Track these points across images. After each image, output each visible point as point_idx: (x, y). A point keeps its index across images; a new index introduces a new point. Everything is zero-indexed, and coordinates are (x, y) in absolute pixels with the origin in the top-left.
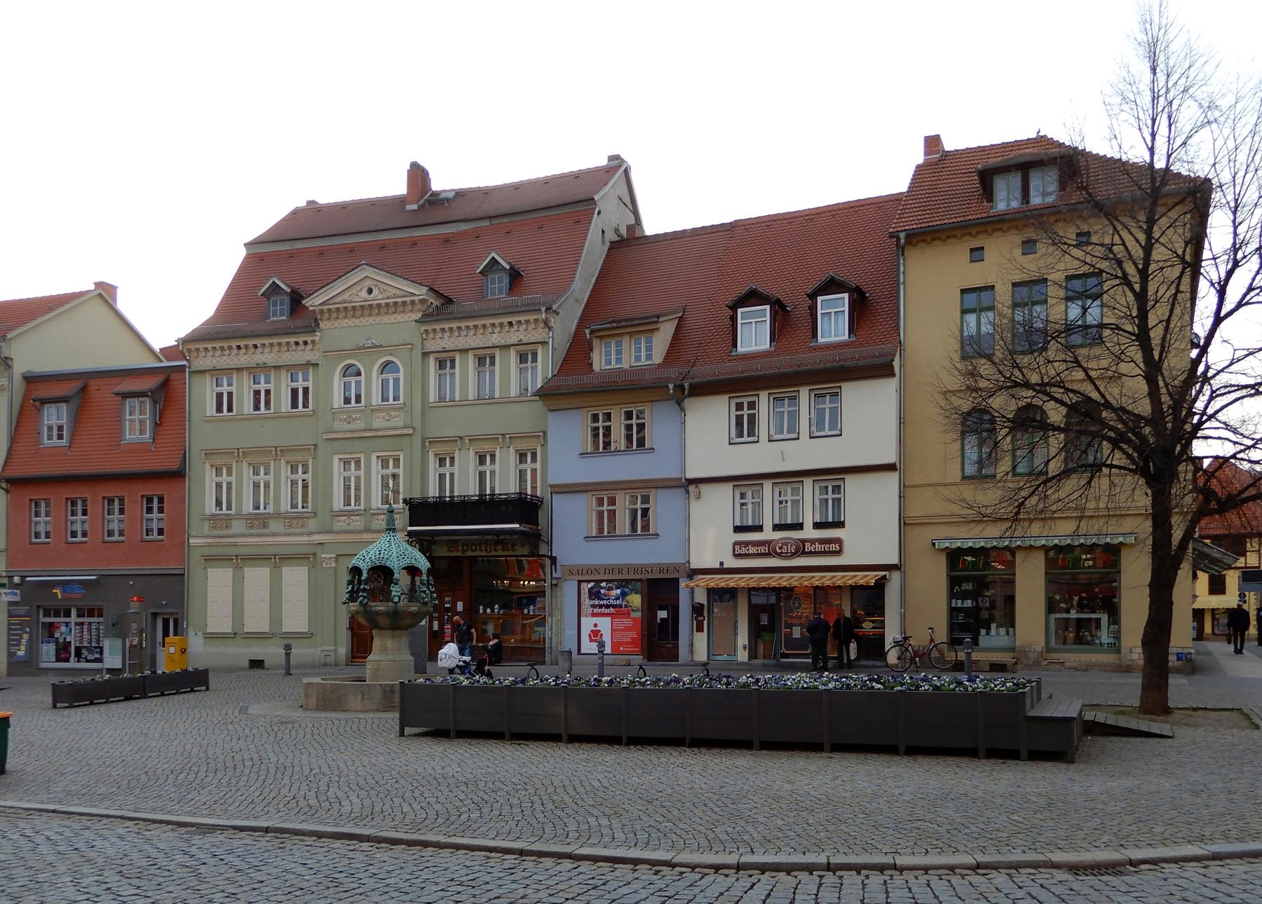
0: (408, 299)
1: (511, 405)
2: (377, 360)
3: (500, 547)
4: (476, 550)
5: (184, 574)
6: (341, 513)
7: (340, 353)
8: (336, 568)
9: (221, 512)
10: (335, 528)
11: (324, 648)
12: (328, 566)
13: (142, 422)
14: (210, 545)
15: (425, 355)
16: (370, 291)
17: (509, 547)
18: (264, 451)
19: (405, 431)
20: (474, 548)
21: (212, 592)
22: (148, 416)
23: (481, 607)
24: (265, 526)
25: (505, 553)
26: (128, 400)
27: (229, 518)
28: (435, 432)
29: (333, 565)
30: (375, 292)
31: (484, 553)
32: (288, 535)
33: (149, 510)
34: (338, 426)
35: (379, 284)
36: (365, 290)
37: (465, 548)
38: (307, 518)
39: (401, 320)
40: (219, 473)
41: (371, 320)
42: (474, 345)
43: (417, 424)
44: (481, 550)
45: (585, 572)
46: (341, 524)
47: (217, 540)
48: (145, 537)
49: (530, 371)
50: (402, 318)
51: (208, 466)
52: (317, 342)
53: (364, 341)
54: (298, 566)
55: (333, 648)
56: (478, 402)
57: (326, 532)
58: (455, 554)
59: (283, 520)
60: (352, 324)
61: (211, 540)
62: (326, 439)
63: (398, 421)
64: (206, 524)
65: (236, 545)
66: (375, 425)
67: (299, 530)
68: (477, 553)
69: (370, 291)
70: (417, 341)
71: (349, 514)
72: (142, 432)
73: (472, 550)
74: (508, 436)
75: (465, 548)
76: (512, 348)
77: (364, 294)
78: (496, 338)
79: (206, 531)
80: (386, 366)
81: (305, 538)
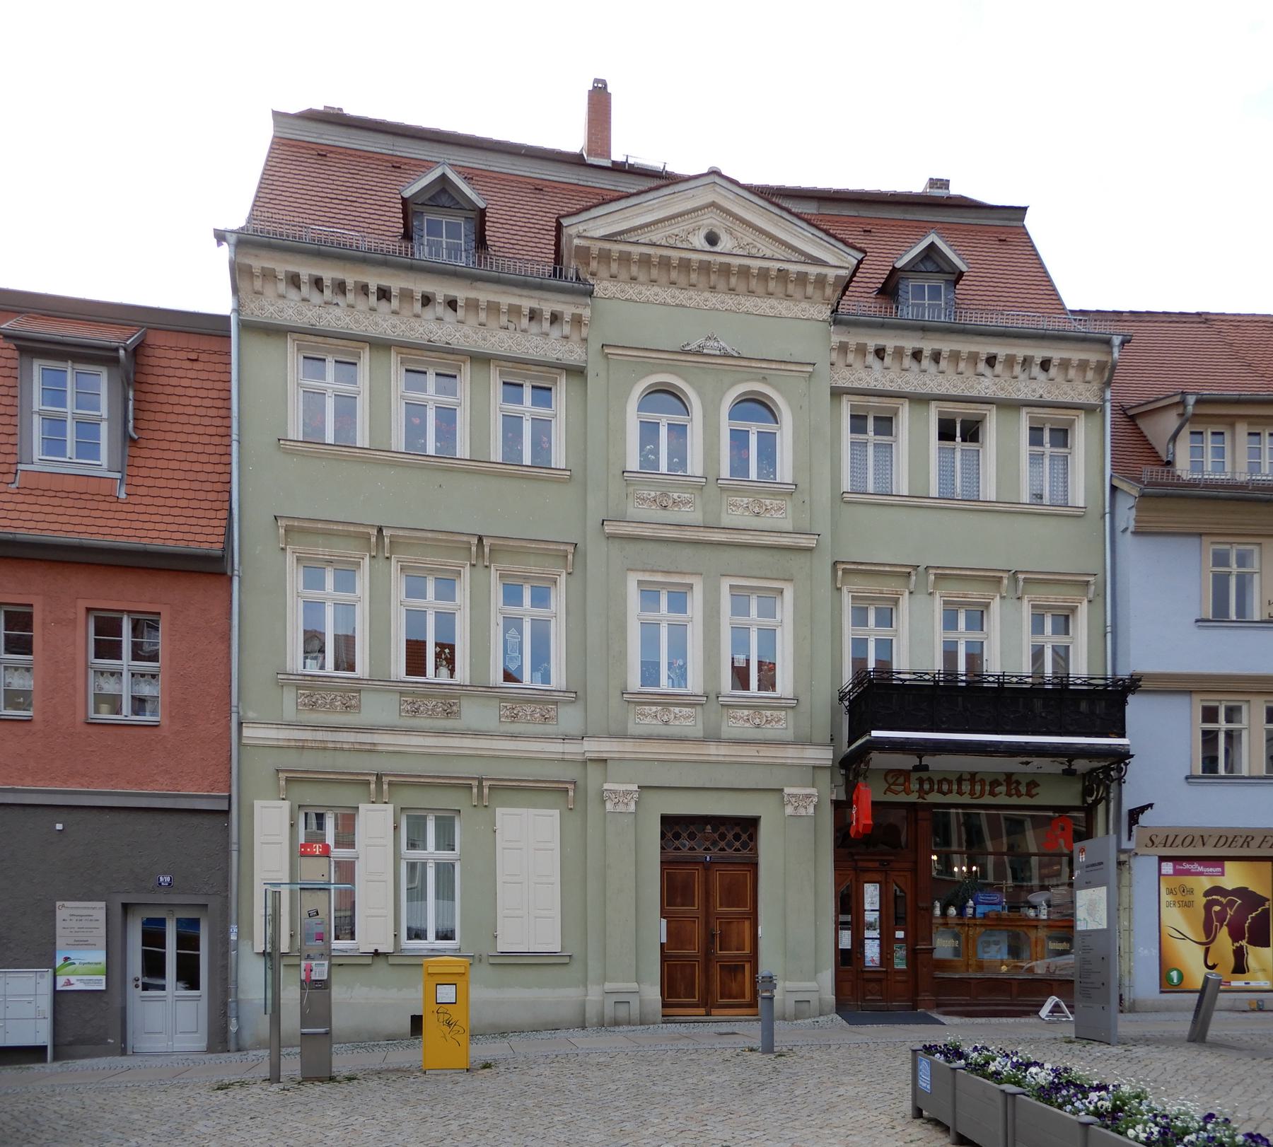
0: (813, 270)
1: (1021, 518)
2: (733, 385)
3: (1003, 789)
4: (950, 791)
5: (227, 813)
6: (640, 700)
7: (648, 355)
8: (635, 813)
9: (321, 673)
10: (632, 729)
11: (609, 986)
12: (621, 808)
13: (87, 428)
14: (301, 747)
15: (837, 393)
16: (712, 239)
17: (1023, 789)
18: (448, 542)
19: (804, 541)
20: (945, 787)
21: (507, 863)
22: (104, 412)
23: (938, 904)
24: (449, 714)
25: (1014, 801)
26: (37, 366)
27: (357, 688)
28: (854, 553)
29: (632, 808)
30: (725, 243)
31: (966, 799)
32: (514, 737)
33: (108, 649)
34: (635, 510)
35: (738, 227)
36: (703, 233)
37: (926, 787)
38: (556, 703)
39: (784, 313)
40: (314, 582)
41: (714, 300)
42: (943, 391)
43: (824, 527)
44: (960, 793)
45: (1179, 841)
46: (647, 719)
47: (320, 735)
48: (92, 714)
49: (1047, 461)
50: (788, 309)
51: (290, 559)
52: (586, 320)
53: (701, 341)
54: (535, 806)
55: (635, 985)
56: (942, 503)
57: (612, 736)
58: (902, 798)
59: (495, 703)
60: (669, 301)
61: (307, 735)
62: (610, 537)
63: (780, 517)
64: (289, 697)
65: (372, 750)
66: (726, 521)
67: (539, 729)
68: (953, 798)
69: (712, 239)
70: (823, 366)
71: (667, 701)
72: (88, 448)
73: (940, 791)
74: (1021, 576)
75: (926, 787)
76: (1024, 411)
77: (699, 241)
78: (987, 385)
79: (289, 712)
80: (756, 405)
81: (556, 748)
